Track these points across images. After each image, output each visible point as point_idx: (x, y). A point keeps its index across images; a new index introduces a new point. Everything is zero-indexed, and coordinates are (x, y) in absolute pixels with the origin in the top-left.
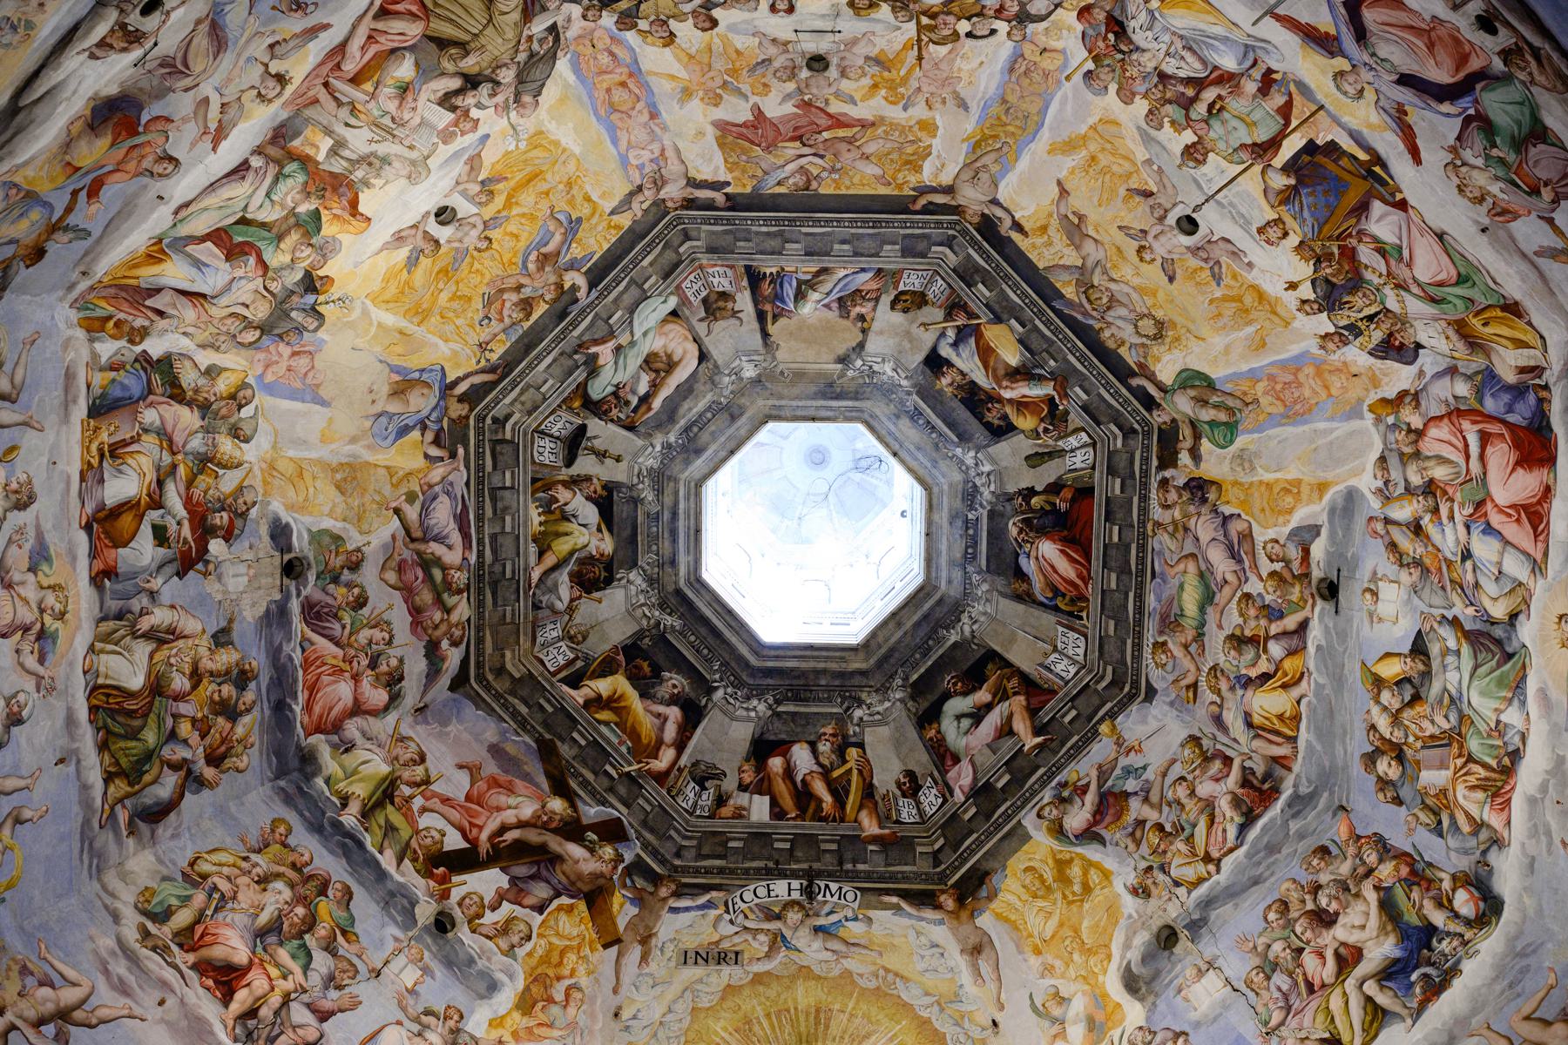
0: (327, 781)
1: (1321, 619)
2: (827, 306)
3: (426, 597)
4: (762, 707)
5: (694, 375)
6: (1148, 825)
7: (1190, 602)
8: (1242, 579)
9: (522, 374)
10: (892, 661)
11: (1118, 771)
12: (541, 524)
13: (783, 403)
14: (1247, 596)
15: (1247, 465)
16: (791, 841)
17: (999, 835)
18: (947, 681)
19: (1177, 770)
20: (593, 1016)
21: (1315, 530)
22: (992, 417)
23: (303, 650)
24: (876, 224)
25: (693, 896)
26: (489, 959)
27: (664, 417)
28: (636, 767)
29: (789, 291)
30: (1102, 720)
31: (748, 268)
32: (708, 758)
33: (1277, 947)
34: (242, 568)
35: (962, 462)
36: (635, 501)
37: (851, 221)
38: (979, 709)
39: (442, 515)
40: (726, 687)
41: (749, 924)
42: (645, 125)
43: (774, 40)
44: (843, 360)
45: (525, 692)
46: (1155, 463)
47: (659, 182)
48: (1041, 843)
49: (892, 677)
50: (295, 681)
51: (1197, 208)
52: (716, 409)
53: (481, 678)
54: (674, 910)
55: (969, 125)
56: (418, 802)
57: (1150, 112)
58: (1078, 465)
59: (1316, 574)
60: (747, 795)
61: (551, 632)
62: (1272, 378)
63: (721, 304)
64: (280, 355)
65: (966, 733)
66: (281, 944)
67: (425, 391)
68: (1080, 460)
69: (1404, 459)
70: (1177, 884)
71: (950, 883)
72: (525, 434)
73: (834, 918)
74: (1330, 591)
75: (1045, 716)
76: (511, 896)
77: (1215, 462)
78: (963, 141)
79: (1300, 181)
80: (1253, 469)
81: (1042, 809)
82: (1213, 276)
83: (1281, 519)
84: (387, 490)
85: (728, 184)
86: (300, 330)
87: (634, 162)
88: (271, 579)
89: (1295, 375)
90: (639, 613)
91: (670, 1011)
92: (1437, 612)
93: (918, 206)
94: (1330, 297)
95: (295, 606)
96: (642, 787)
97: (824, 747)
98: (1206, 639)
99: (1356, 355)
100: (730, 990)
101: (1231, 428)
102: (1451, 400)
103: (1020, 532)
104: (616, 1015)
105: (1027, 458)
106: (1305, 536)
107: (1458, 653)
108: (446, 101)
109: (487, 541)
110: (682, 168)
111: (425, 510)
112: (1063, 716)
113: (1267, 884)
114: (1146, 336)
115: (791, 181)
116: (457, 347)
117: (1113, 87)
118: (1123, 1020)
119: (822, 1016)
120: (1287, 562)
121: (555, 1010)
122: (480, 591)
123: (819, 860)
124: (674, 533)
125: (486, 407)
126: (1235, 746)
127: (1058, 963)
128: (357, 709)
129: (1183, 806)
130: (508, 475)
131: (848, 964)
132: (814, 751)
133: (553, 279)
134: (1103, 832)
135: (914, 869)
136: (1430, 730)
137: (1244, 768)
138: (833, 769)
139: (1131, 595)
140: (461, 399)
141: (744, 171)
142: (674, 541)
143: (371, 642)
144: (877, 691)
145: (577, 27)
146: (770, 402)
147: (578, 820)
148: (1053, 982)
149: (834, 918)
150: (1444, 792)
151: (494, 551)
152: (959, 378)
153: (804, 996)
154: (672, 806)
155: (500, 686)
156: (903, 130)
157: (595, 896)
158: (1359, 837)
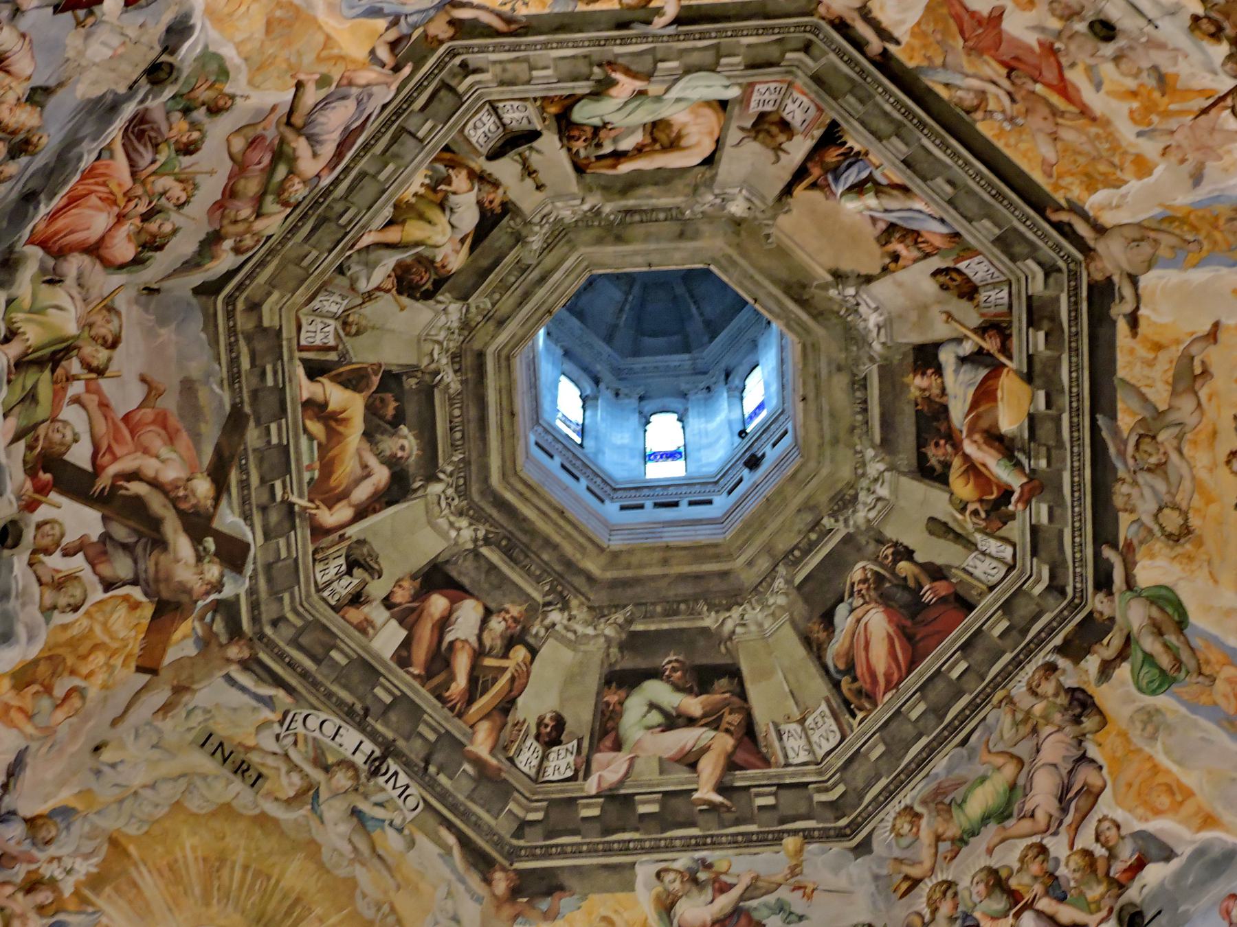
2: (874, 220)
3: (251, 186)
4: (467, 534)
5: (684, 171)
7: (979, 801)
8: (1052, 828)
10: (630, 592)
11: (771, 899)
12: (415, 195)
13: (743, 262)
14: (1043, 850)
15: (1150, 729)
16: (395, 698)
18: (669, 660)
20: (74, 734)
21: (1168, 854)
23: (98, 158)
24: (999, 196)
26: (24, 605)
27: (619, 185)
29: (852, 177)
30: (795, 832)
31: (834, 125)
32: (376, 545)
34: (115, 41)
35: (864, 464)
36: (519, 239)
37: (978, 173)
38: (679, 716)
40: (449, 486)
41: (293, 754)
44: (839, 276)
45: (260, 346)
46: (1058, 640)
49: (618, 607)
50: (65, 182)
52: (674, 215)
53: (231, 300)
55: (1183, 199)
56: (77, 388)
58: (977, 573)
59: (1133, 894)
60: (386, 614)
61: (332, 304)
63: (774, 130)
65: (649, 728)
68: (985, 570)
71: (519, 865)
72: (479, 98)
73: (379, 813)
75: (740, 779)
76: (91, 552)
78: (1161, 205)
80: (1153, 737)
81: (667, 870)
83: (1140, 811)
84: (309, 58)
85: (898, 43)
88: (133, 69)
90: (427, 347)
91: (153, 786)
93: (1055, 217)
95: (129, 110)
96: (294, 528)
97: (497, 625)
98: (965, 850)
100: (226, 811)
101: (1165, 681)
104: (97, 749)
105: (932, 519)
109: (353, 173)
111: (325, 103)
112: (758, 795)
114: (1162, 528)
115: (960, 93)
119: (298, 910)
120: (1112, 856)
121: (45, 703)
122: (304, 217)
123: (408, 738)
124: (526, 296)
128: (94, 250)
130: (429, 125)
131: (363, 876)
132: (484, 622)
135: (492, 822)
138: (489, 654)
139: (924, 741)
140: (452, 22)
141: (925, 46)
142: (520, 304)
144: (590, 608)
147: (210, 518)
149: (379, 813)
151: (351, 189)
152: (936, 391)
154: (306, 569)
155: (244, 322)
156: (1116, 147)
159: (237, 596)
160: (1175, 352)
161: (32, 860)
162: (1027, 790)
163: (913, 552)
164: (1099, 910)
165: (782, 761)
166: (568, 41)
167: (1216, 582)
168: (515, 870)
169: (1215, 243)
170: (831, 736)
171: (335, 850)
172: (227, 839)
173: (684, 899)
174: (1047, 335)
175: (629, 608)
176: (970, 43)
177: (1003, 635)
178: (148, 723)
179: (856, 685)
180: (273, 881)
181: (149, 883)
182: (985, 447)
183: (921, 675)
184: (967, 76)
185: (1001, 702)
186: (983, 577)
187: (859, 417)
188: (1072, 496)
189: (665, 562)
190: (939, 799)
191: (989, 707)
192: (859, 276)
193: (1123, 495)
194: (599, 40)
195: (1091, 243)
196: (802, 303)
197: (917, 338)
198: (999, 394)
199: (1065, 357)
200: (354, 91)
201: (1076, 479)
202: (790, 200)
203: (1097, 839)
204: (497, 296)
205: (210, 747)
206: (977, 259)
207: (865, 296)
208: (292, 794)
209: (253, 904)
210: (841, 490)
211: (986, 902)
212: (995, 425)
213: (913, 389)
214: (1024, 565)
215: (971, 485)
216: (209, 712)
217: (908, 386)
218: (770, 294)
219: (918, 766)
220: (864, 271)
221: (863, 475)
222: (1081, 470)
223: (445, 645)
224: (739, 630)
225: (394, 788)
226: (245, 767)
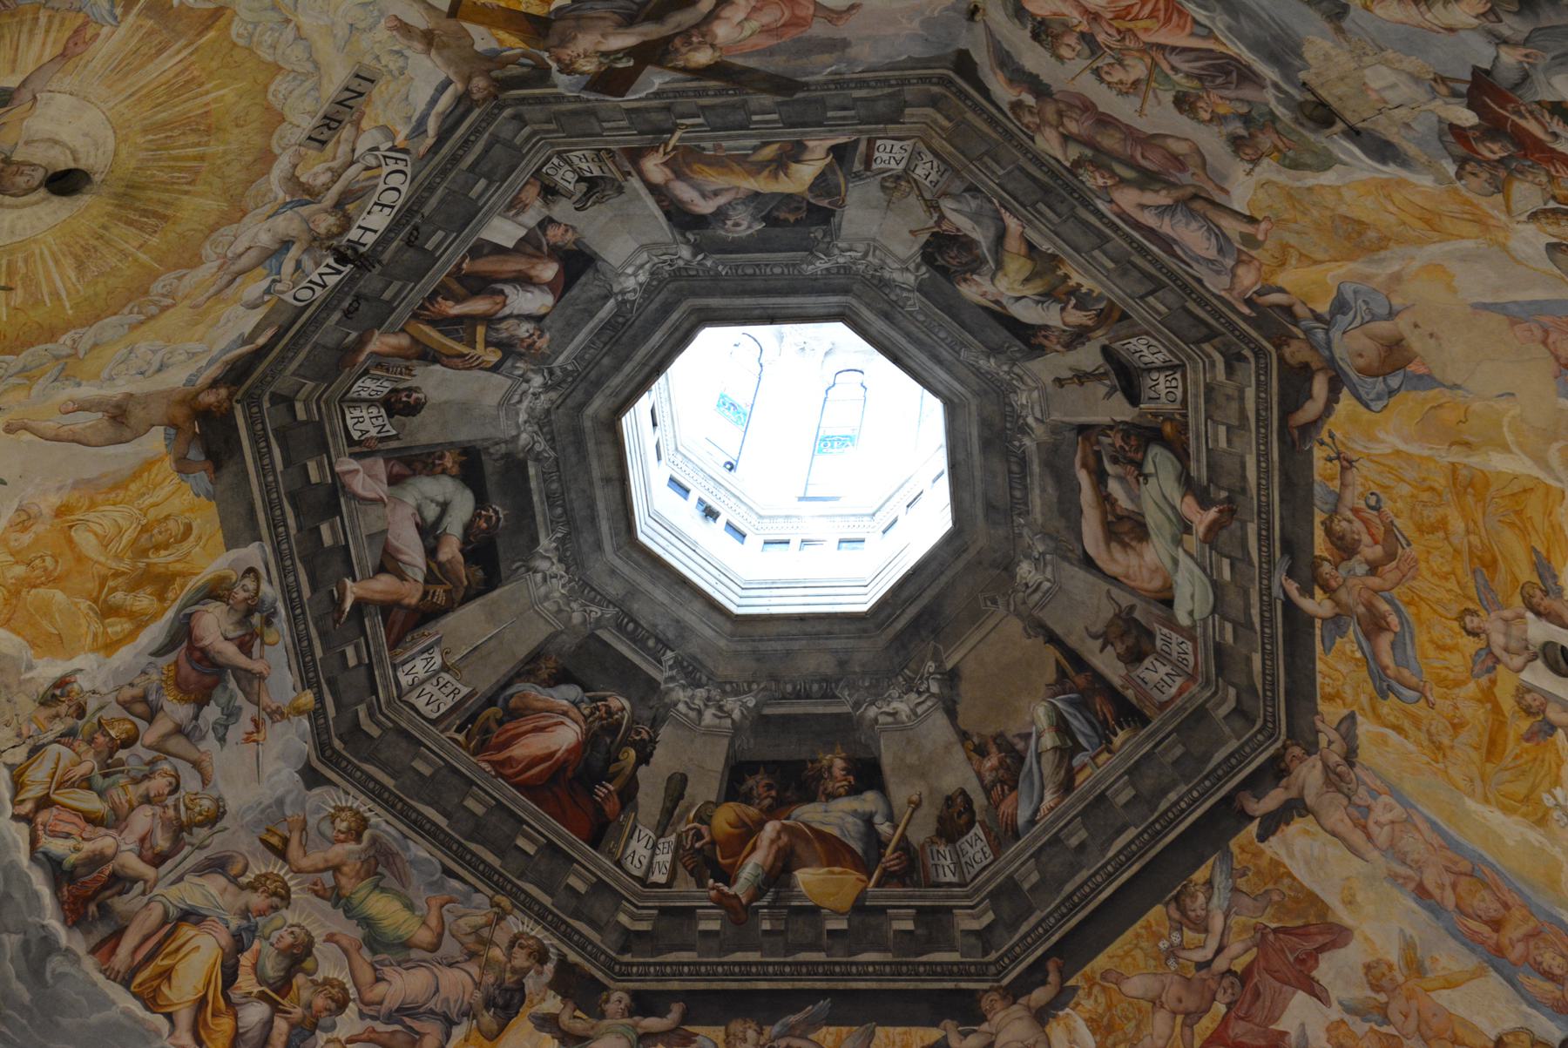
2: (1027, 736)
3: (1110, 141)
5: (1079, 537)
6: (142, 724)
7: (384, 908)
9: (1264, 440)
10: (571, 449)
11: (240, 699)
12: (1067, 277)
13: (960, 564)
14: (341, 1005)
18: (499, 511)
19: (191, 783)
25: (446, 116)
28: (672, 143)
29: (1077, 723)
30: (319, 698)
32: (616, 201)
35: (737, 693)
36: (993, 351)
37: (1097, 890)
38: (437, 538)
39: (1192, 236)
42: (1419, 867)
44: (951, 678)
46: (573, 957)
49: (552, 441)
52: (1019, 506)
53: (944, 81)
58: (634, 843)
60: (532, 223)
63: (1130, 641)
65: (419, 509)
67: (1361, 362)
68: (638, 849)
70: (35, 750)
72: (1189, 357)
73: (288, 266)
85: (1262, 838)
87: (1385, 799)
91: (299, 37)
93: (1051, 966)
96: (641, 133)
97: (525, 329)
98: (327, 905)
103: (610, 713)
105: (684, 779)
110: (1329, 824)
115: (1201, 898)
116: (1378, 449)
119: (153, 221)
123: (381, 274)
126: (172, 877)
127: (27, 538)
129: (136, 782)
132: (529, 318)
133: (1343, 595)
134: (172, 657)
135: (288, 372)
137: (135, 880)
138: (489, 328)
141: (1259, 873)
142: (908, 335)
143: (1120, 62)
144: (548, 412)
146: (972, 552)
149: (288, 266)
152: (830, 786)
159: (555, 86)
162: (407, 965)
163: (647, 763)
165: (398, 661)
166: (1269, 478)
168: (232, 408)
170: (433, 707)
171: (236, 237)
172: (236, 131)
173: (224, 607)
174: (910, 932)
175: (552, 454)
176: (1271, 937)
177: (570, 888)
179: (493, 725)
180: (186, 188)
181: (168, 64)
182: (775, 847)
183: (514, 800)
184: (1226, 917)
185: (498, 905)
186: (629, 851)
187: (789, 688)
188: (735, 964)
190: (382, 859)
191: (490, 893)
192: (955, 702)
193: (744, 1032)
194: (1269, 512)
195: (1023, 1000)
196: (916, 624)
197: (887, 761)
198: (837, 869)
199: (889, 957)
200: (1229, 262)
201: (754, 969)
202: (1041, 639)
204: (921, 318)
205: (355, 85)
206: (987, 849)
207: (929, 703)
208: (303, 179)
209: (153, 176)
210: (704, 667)
211: (272, 952)
213: (829, 757)
214: (648, 898)
215: (728, 829)
216: (402, 73)
217: (832, 751)
218: (922, 590)
219: (415, 822)
220: (960, 708)
221: (724, 692)
222: (765, 977)
223: (499, 286)
224: (539, 576)
225: (321, 275)
226: (333, 125)
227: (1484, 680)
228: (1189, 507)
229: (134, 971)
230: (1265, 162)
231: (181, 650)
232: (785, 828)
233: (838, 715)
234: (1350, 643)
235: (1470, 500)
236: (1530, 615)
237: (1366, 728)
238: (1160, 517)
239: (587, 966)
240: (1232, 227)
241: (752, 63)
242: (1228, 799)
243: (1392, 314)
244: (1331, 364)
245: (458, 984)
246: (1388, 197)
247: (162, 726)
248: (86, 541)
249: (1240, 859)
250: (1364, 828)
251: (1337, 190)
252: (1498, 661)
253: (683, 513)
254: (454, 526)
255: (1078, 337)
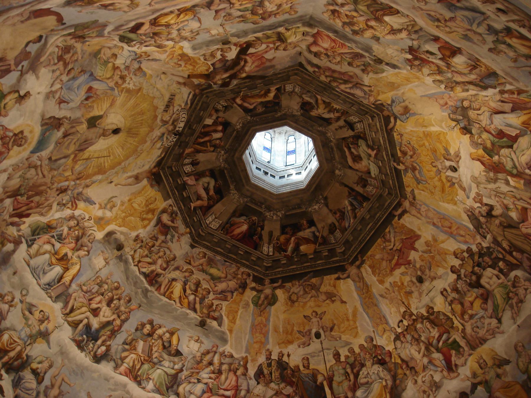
0: (298, 27)
1: (196, 318)
3: (336, 75)
6: (155, 242)
7: (213, 271)
8: (215, 292)
9: (383, 134)
11: (174, 233)
14: (209, 293)
17: (169, 190)
18: (220, 182)
19: (168, 252)
21: (220, 325)
22: (288, 229)
23: (349, 47)
24: (361, 242)
25: (191, 100)
28: (241, 94)
29: (355, 203)
30: (190, 229)
33: (106, 287)
35: (280, 211)
36: (320, 126)
37: (366, 238)
39: (358, 92)
42: (432, 219)
43: (435, 278)
44: (326, 199)
46: (256, 274)
47: (412, 204)
48: (162, 204)
51: (322, 343)
53: (297, 69)
54: (190, 93)
55: (374, 291)
56: (271, 46)
57: (354, 352)
58: (264, 248)
59: (208, 321)
62: (265, 326)
64: (450, 101)
66: (253, 6)
67: (400, 113)
68: (265, 249)
69: (230, 364)
70: (135, 251)
73: (165, 139)
74: (202, 324)
77: (250, 294)
79: (317, 386)
80: (243, 308)
82: (301, 331)
83: (227, 313)
85: (399, 219)
86: (454, 113)
87: (423, 206)
89: (263, 334)
91: (158, 90)
92: (186, 364)
93: (359, 256)
94: (282, 365)
96: (234, 94)
98: (201, 273)
99: (262, 359)
100: (156, 108)
101: (256, 304)
102: (241, 388)
103: (253, 220)
104: (164, 73)
106: (219, 320)
107: (173, 369)
108: (491, 208)
113: (126, 282)
114: (291, 295)
115: (388, 235)
116: (407, 131)
117: (366, 345)
118: (99, 231)
120: (214, 311)
121: (176, 61)
125: (380, 118)
127: (124, 207)
129: (157, 254)
131: (148, 143)
133: (406, 164)
134: (158, 227)
136: (155, 349)
137: (161, 274)
139: (222, 251)
143: (334, 58)
144: (226, 158)
145: (479, 239)
148: (118, 205)
149: (165, 139)
150: (135, 349)
153: (143, 130)
157: (207, 76)
158: (130, 312)
160: (335, 292)
161: (129, 74)
162: (221, 282)
164: (202, 314)
167: (284, 312)
169: (365, 299)
177: (252, 260)
178: (174, 81)
181: (132, 102)
183: (236, 243)
189: (242, 171)
194: (387, 149)
196: (316, 188)
199: (324, 261)
200: (367, 96)
203: (216, 305)
212: (301, 245)
221: (277, 212)
222: (298, 270)
227: (439, 176)
228: (370, 151)
229: (165, 293)
230: (370, 74)
231: (160, 225)
232: (296, 238)
233: (302, 212)
234: (410, 174)
235: (428, 138)
236: (445, 160)
237: (416, 192)
238: (364, 155)
239: (260, 276)
240: (366, 89)
241: (255, 74)
242: (390, 213)
243: (404, 101)
244: (394, 114)
245: (232, 284)
246: (398, 76)
247: (159, 241)
248: (135, 205)
249: (395, 225)
250: (420, 213)
251: (386, 77)
252: (441, 172)
253: (260, 174)
254: (212, 186)
255: (338, 119)
